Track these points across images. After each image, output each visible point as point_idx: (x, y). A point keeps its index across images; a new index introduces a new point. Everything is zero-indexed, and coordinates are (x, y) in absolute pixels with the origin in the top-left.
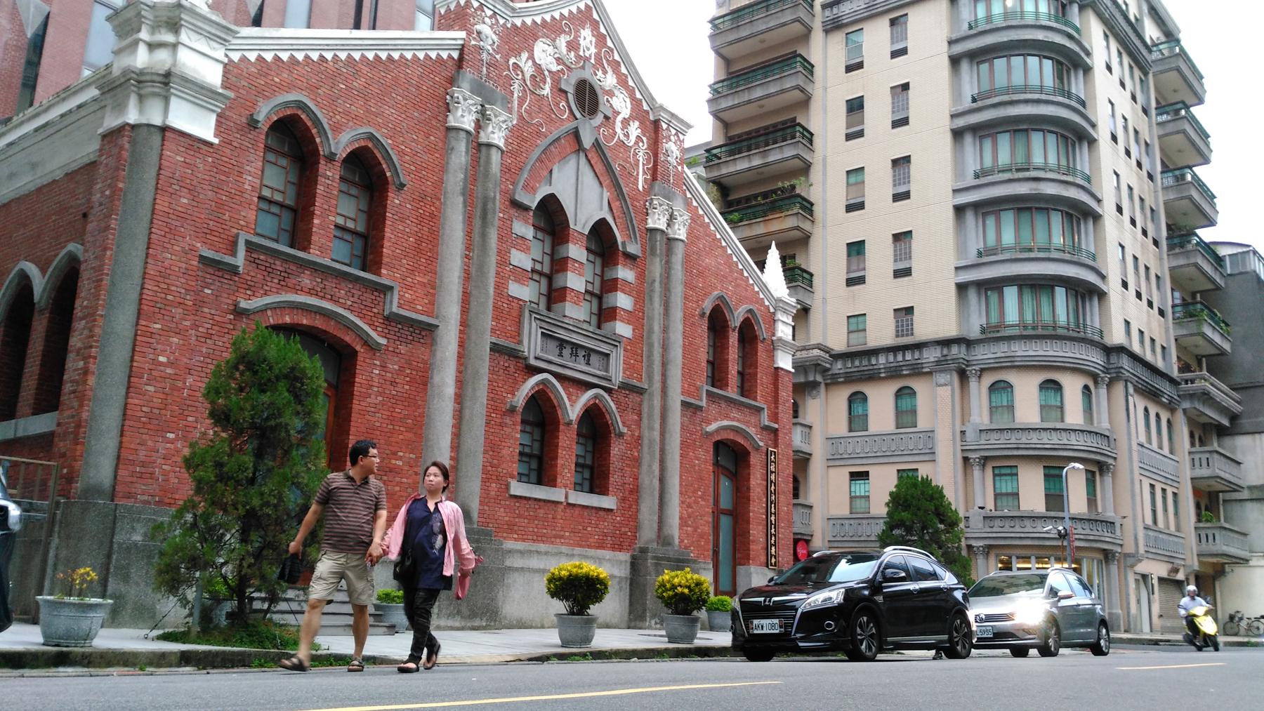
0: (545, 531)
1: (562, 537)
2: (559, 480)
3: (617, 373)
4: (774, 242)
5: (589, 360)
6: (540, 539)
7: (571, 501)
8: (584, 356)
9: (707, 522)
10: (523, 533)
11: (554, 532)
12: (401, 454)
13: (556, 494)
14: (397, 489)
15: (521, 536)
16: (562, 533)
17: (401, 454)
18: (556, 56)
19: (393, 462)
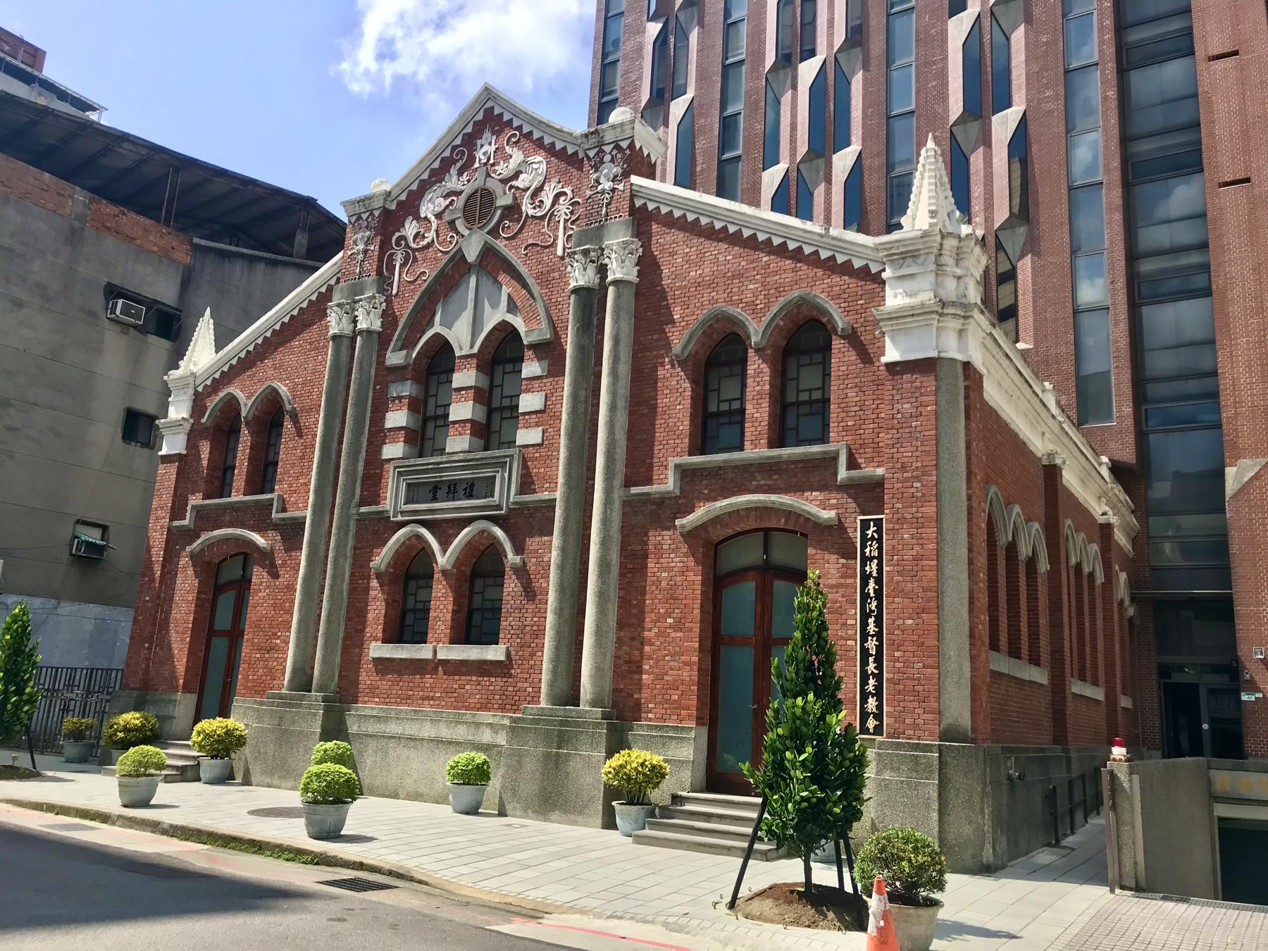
0: (411, 693)
1: (432, 698)
2: (430, 635)
3: (506, 493)
4: (930, 135)
5: (472, 491)
6: (404, 701)
7: (440, 656)
8: (465, 489)
9: (686, 664)
10: (386, 696)
11: (421, 693)
12: (279, 634)
13: (423, 652)
14: (275, 663)
15: (383, 700)
16: (431, 694)
17: (279, 634)
18: (444, 194)
19: (274, 641)
